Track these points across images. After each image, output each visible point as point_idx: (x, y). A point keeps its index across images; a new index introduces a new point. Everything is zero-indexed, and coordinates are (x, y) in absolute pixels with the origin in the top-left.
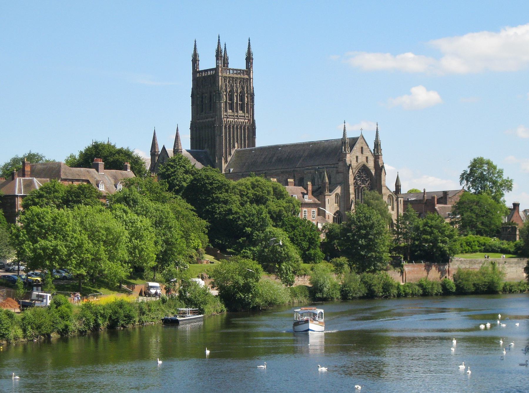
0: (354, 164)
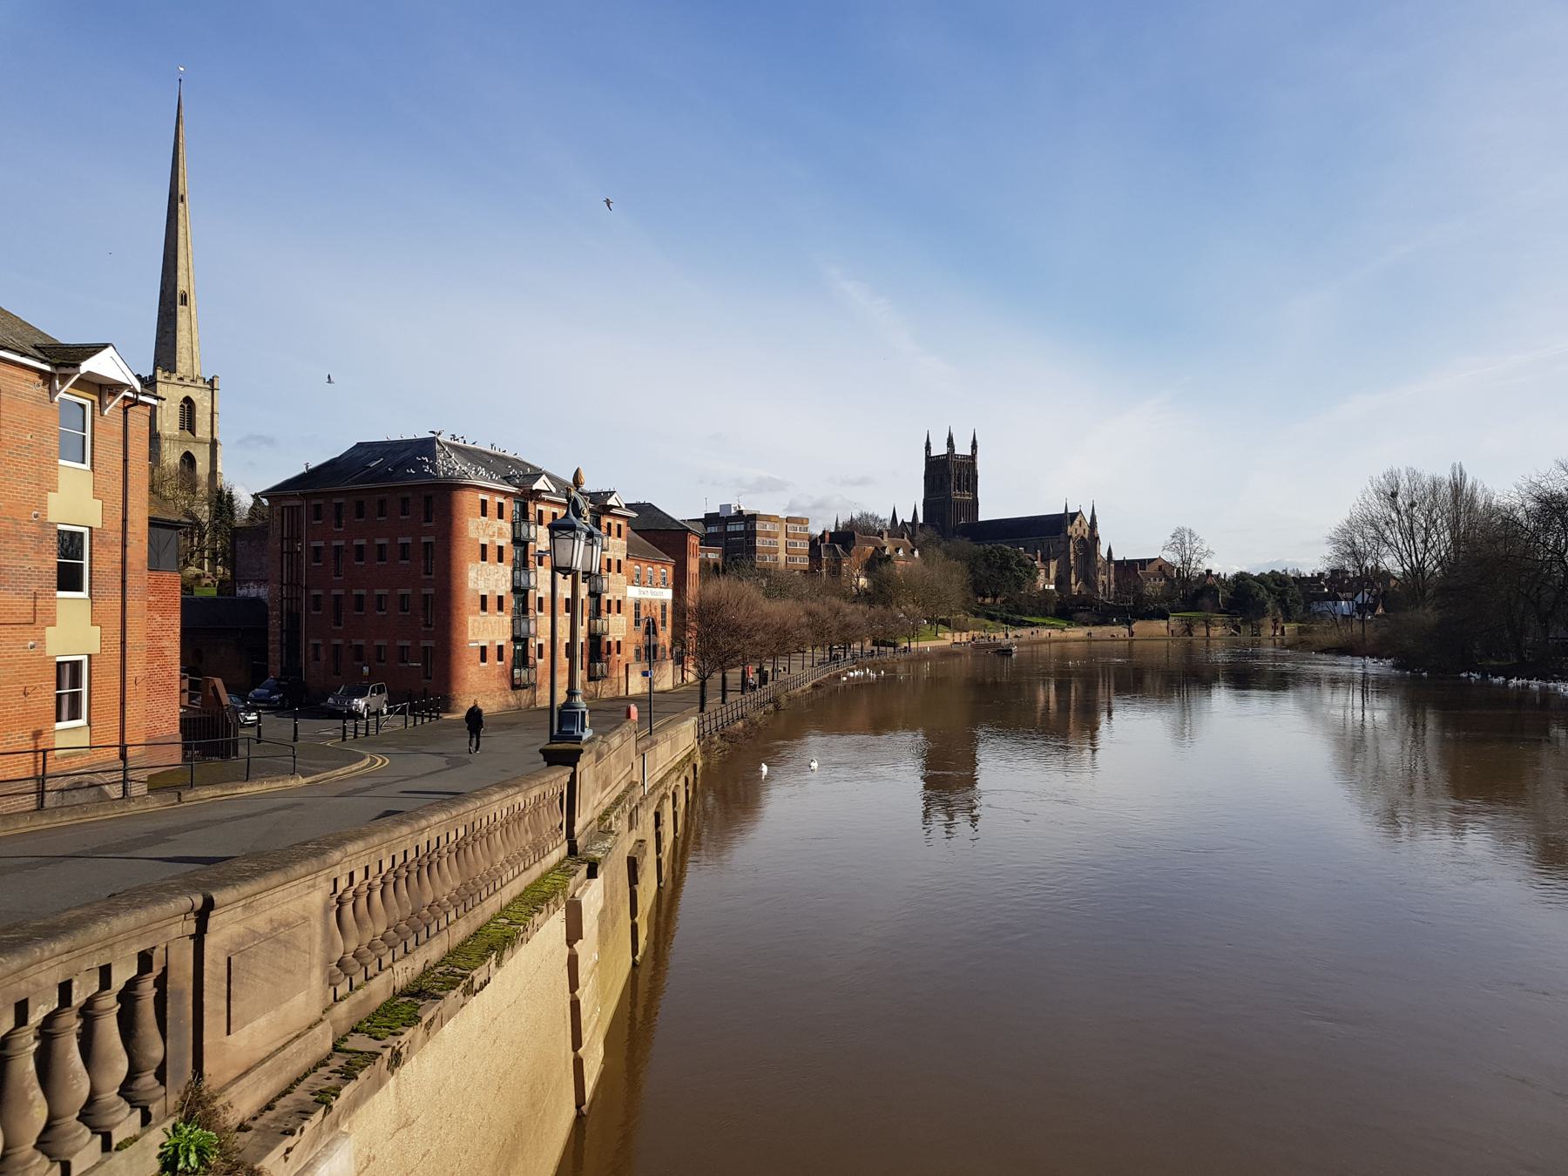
0: (1074, 535)
